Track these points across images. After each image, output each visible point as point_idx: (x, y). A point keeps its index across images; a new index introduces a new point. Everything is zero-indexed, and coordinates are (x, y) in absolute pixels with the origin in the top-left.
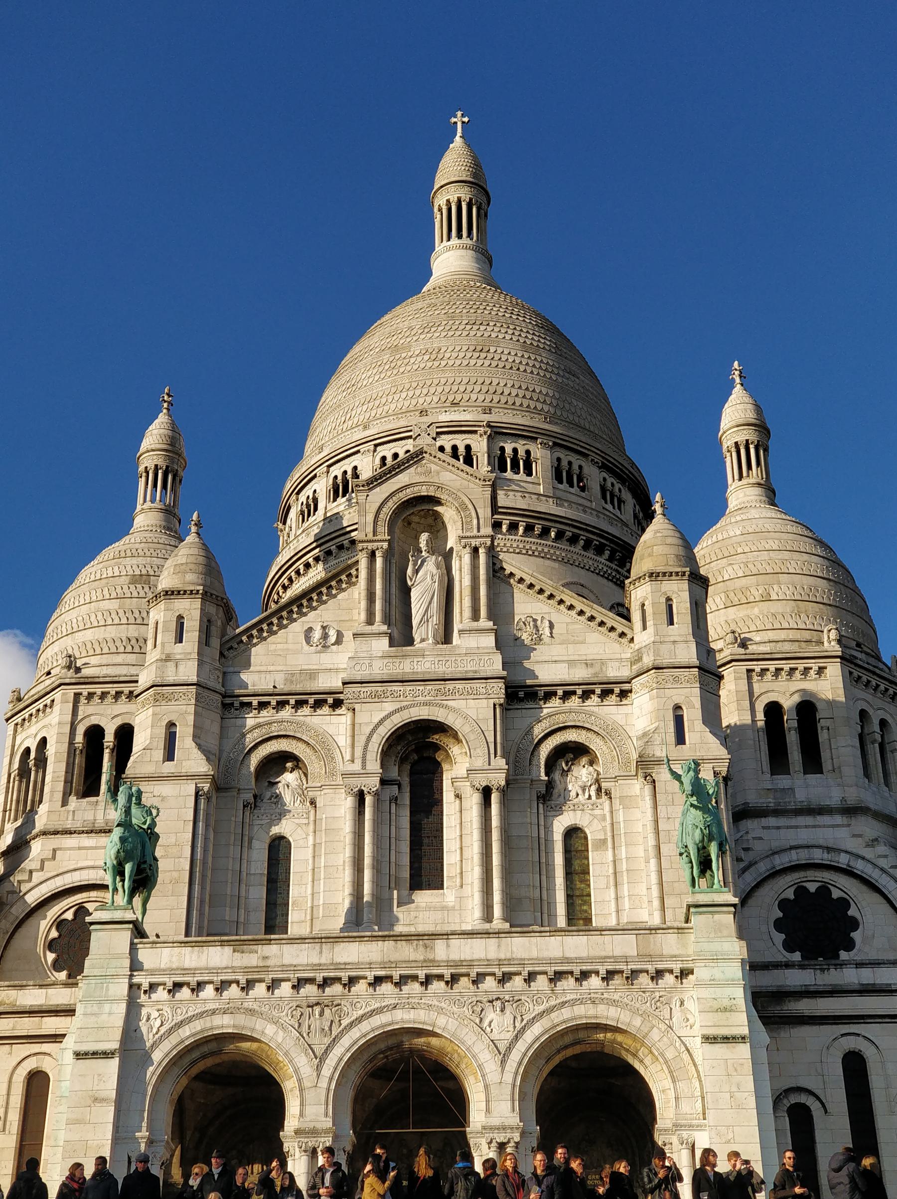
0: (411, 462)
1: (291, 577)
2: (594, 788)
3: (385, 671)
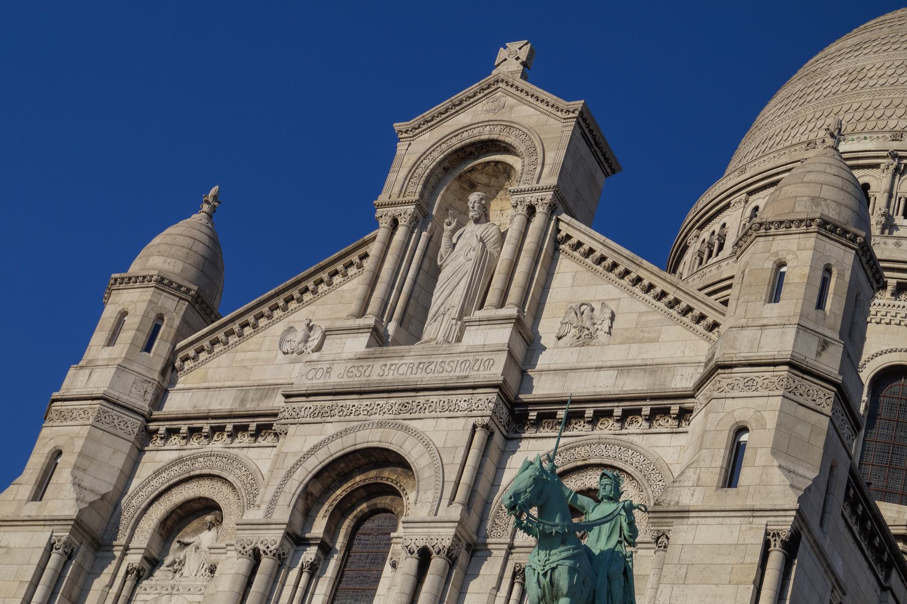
0: (480, 96)
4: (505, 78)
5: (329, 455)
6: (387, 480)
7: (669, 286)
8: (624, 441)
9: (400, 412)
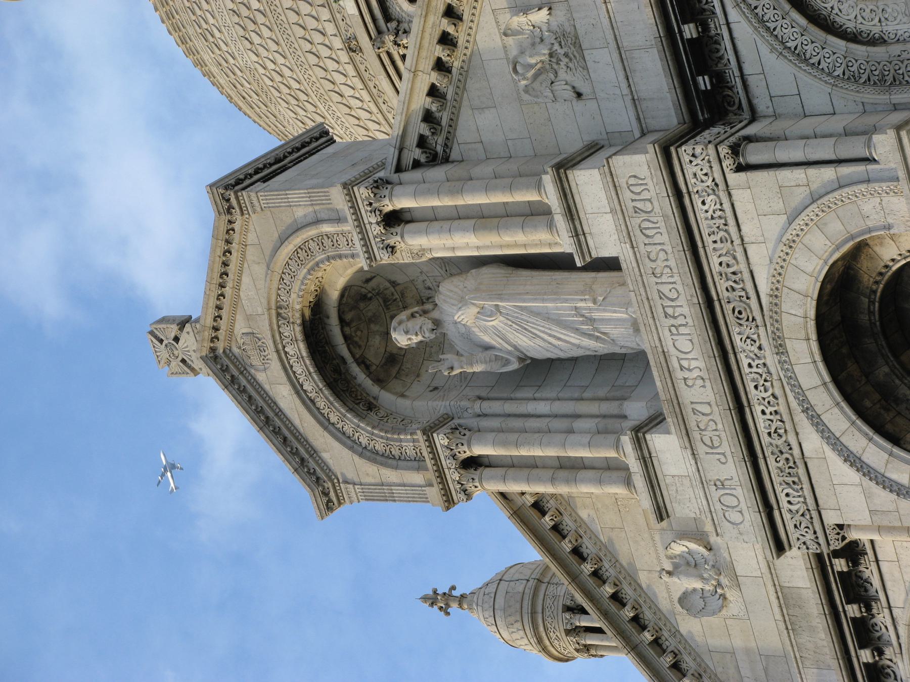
0: (244, 382)
3: (725, 448)
4: (208, 345)
5: (852, 429)
6: (873, 313)
9: (751, 319)
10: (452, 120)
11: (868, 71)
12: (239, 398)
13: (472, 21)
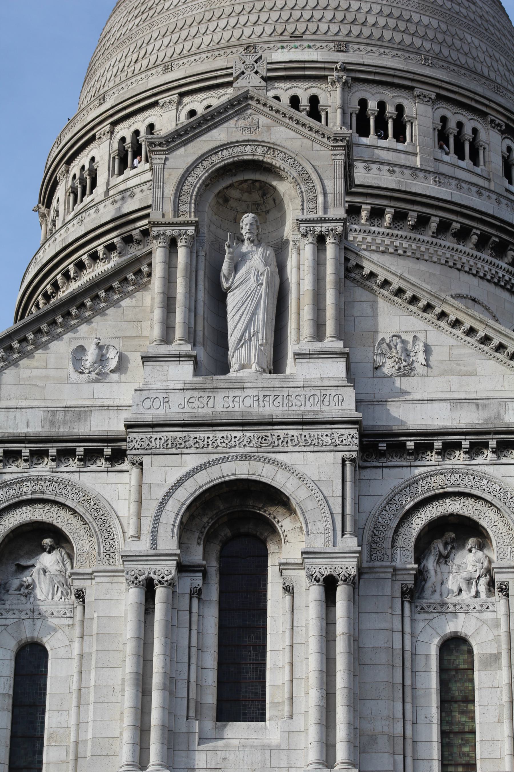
1: (56, 281)
2: (483, 581)
3: (187, 410)
4: (256, 97)
6: (253, 508)
7: (478, 323)
8: (477, 471)
9: (261, 445)
10: (369, 287)
11: (380, 536)
12: (222, 107)
13: (422, 317)
